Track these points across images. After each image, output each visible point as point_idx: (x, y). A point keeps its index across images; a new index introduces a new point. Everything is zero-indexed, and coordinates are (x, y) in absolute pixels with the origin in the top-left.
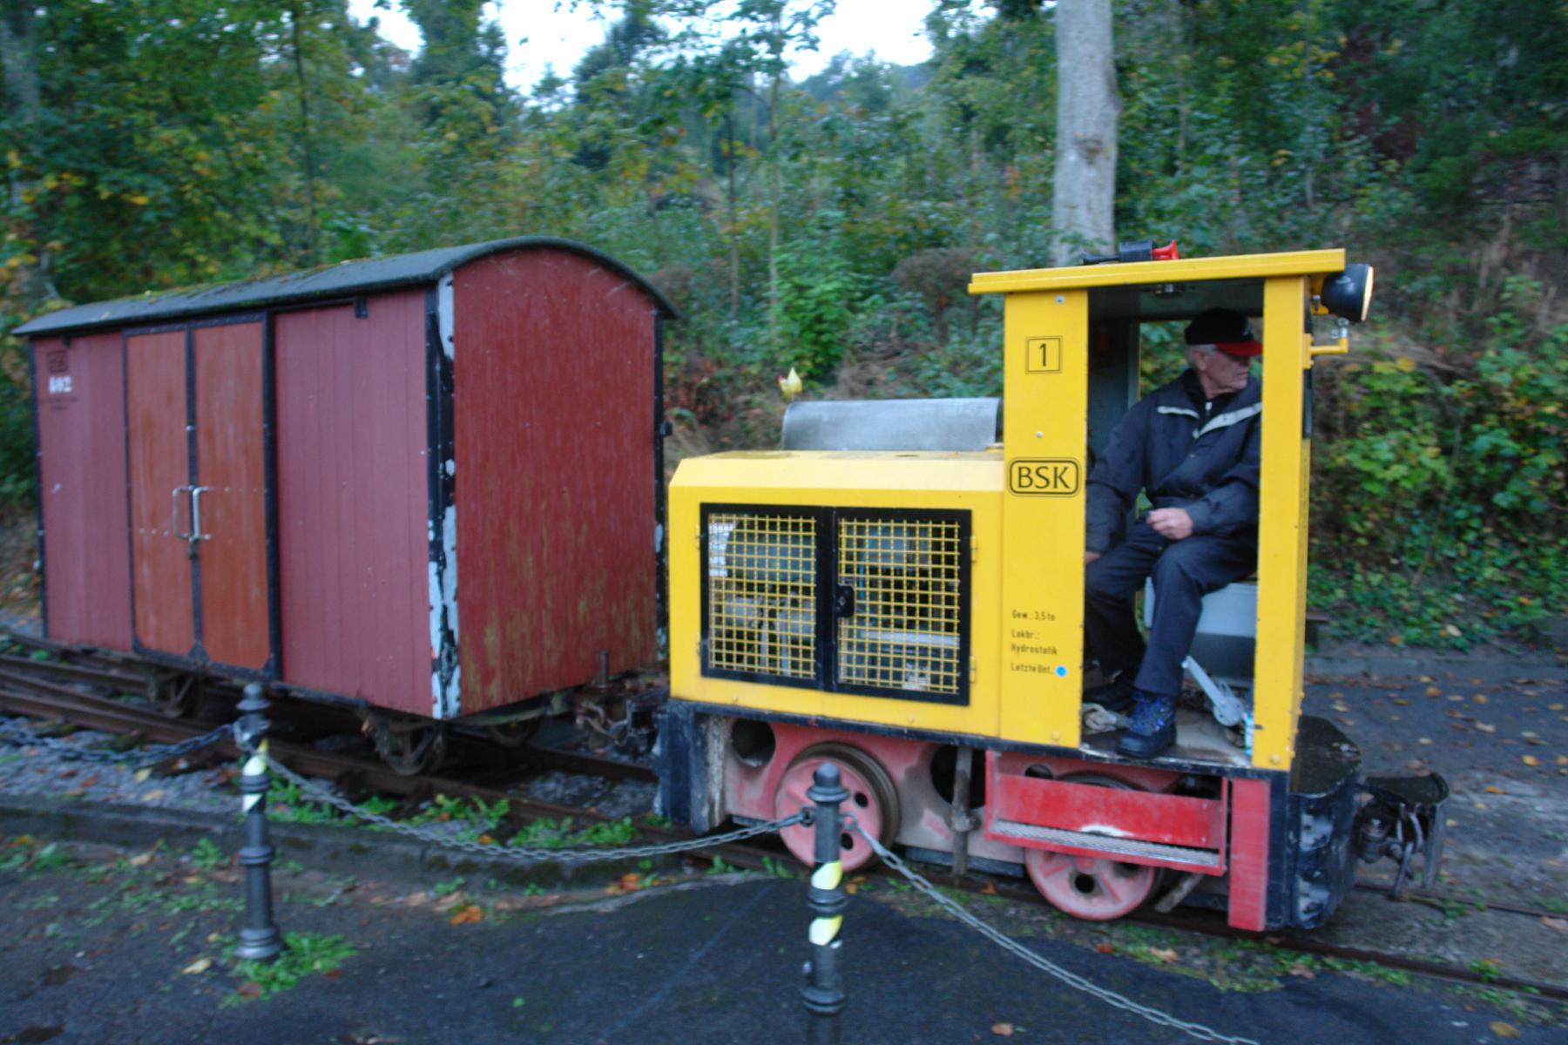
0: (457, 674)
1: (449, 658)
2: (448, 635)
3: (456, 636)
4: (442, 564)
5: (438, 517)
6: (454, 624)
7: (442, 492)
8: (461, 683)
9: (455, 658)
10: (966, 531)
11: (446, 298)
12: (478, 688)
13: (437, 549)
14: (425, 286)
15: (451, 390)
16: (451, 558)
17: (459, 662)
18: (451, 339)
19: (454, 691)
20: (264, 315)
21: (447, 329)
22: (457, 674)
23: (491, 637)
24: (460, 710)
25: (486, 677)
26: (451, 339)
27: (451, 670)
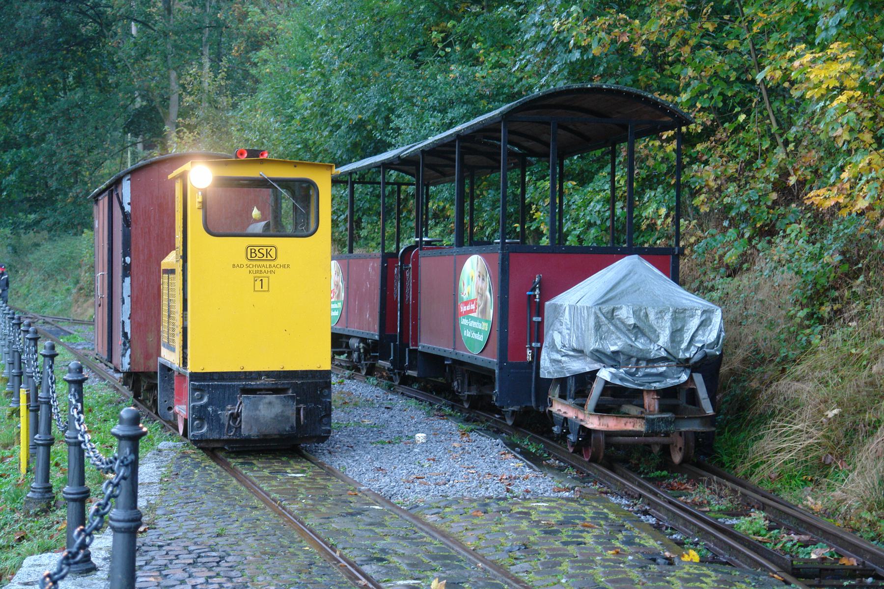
0: (129, 352)
1: (124, 344)
2: (125, 335)
3: (129, 335)
4: (123, 303)
5: (123, 281)
6: (128, 329)
12: (142, 361)
16: (128, 301)
17: (130, 347)
18: (129, 204)
19: (127, 360)
21: (127, 198)
22: (129, 352)
24: (129, 369)
26: (129, 204)
27: (126, 350)
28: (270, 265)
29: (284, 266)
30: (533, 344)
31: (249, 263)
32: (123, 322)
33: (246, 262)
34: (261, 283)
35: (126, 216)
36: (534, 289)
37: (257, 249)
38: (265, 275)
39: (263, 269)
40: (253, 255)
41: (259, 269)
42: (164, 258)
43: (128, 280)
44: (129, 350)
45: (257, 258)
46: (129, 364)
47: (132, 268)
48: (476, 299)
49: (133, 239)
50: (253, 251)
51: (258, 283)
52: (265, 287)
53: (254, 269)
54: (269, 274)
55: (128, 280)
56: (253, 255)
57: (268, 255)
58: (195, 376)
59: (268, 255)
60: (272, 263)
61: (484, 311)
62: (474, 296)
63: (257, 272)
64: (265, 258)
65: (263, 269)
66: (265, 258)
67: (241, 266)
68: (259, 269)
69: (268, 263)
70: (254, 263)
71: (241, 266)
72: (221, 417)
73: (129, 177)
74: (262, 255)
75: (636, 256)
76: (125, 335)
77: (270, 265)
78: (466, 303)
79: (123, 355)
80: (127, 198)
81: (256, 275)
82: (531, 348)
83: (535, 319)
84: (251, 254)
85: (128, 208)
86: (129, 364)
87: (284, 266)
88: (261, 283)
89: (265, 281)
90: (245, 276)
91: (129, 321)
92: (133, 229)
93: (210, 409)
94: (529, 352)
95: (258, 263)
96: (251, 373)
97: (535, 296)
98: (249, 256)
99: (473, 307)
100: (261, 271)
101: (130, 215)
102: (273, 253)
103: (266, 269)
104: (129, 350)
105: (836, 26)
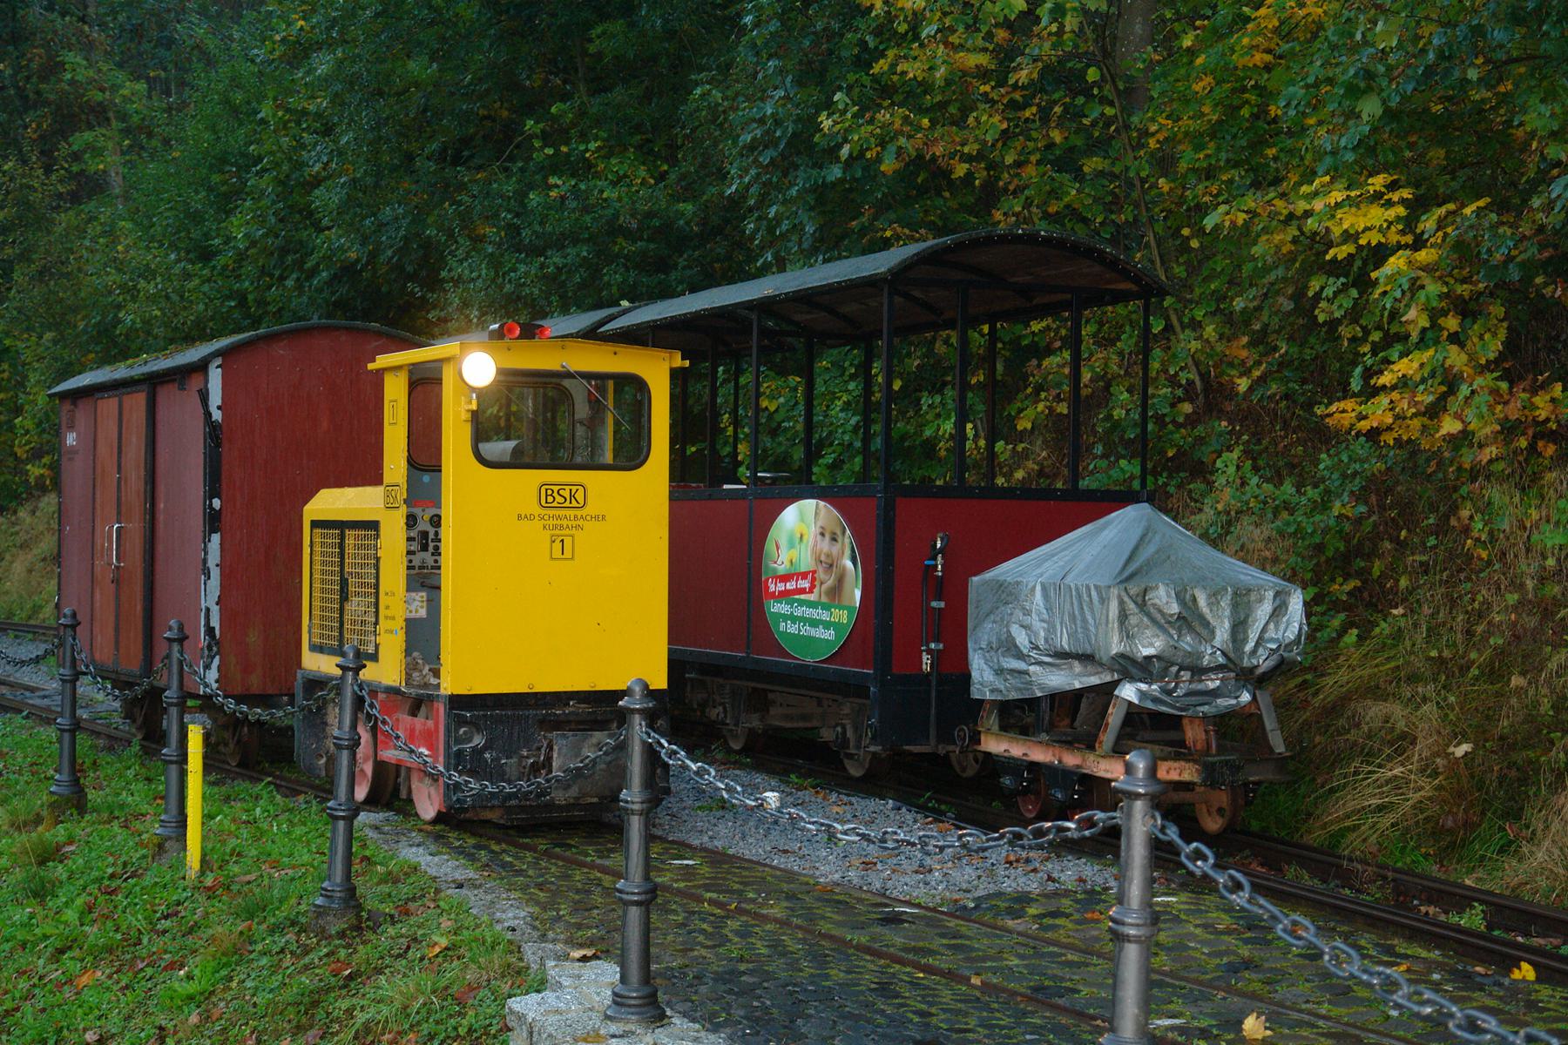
1: (210, 647)
2: (210, 631)
5: (206, 540)
6: (215, 622)
7: (214, 521)
8: (219, 668)
9: (215, 649)
10: (377, 536)
11: (215, 377)
13: (205, 561)
14: (202, 367)
15: (218, 445)
16: (215, 573)
18: (219, 408)
19: (212, 675)
20: (144, 387)
21: (215, 398)
23: (254, 638)
25: (247, 669)
26: (219, 408)
28: (575, 516)
29: (596, 518)
30: (933, 646)
31: (543, 512)
32: (208, 610)
33: (538, 510)
34: (561, 545)
35: (214, 433)
36: (935, 558)
37: (556, 488)
38: (567, 532)
39: (565, 522)
40: (550, 499)
41: (559, 522)
42: (306, 503)
43: (216, 538)
44: (218, 657)
45: (555, 504)
46: (217, 681)
47: (223, 519)
48: (814, 572)
49: (225, 467)
50: (549, 492)
51: (558, 545)
52: (568, 554)
53: (551, 522)
54: (574, 531)
55: (216, 538)
56: (550, 499)
57: (573, 500)
58: (457, 702)
59: (573, 500)
60: (579, 513)
61: (836, 592)
62: (806, 564)
63: (555, 527)
64: (567, 504)
65: (565, 522)
66: (567, 504)
67: (530, 517)
68: (559, 522)
69: (572, 513)
70: (552, 512)
71: (530, 517)
72: (508, 770)
73: (219, 361)
74: (558, 499)
75: (1146, 505)
76: (210, 631)
77: (575, 516)
78: (785, 578)
79: (207, 667)
80: (215, 398)
81: (557, 532)
82: (929, 651)
83: (934, 604)
84: (547, 497)
85: (217, 415)
86: (217, 681)
87: (596, 518)
88: (561, 545)
89: (568, 541)
90: (536, 535)
91: (217, 608)
92: (224, 450)
93: (487, 755)
94: (925, 657)
95: (562, 512)
96: (544, 694)
97: (936, 566)
98: (543, 502)
99: (805, 584)
100: (562, 526)
101: (220, 426)
102: (580, 496)
103: (570, 523)
104: (218, 657)
105: (1354, 149)
